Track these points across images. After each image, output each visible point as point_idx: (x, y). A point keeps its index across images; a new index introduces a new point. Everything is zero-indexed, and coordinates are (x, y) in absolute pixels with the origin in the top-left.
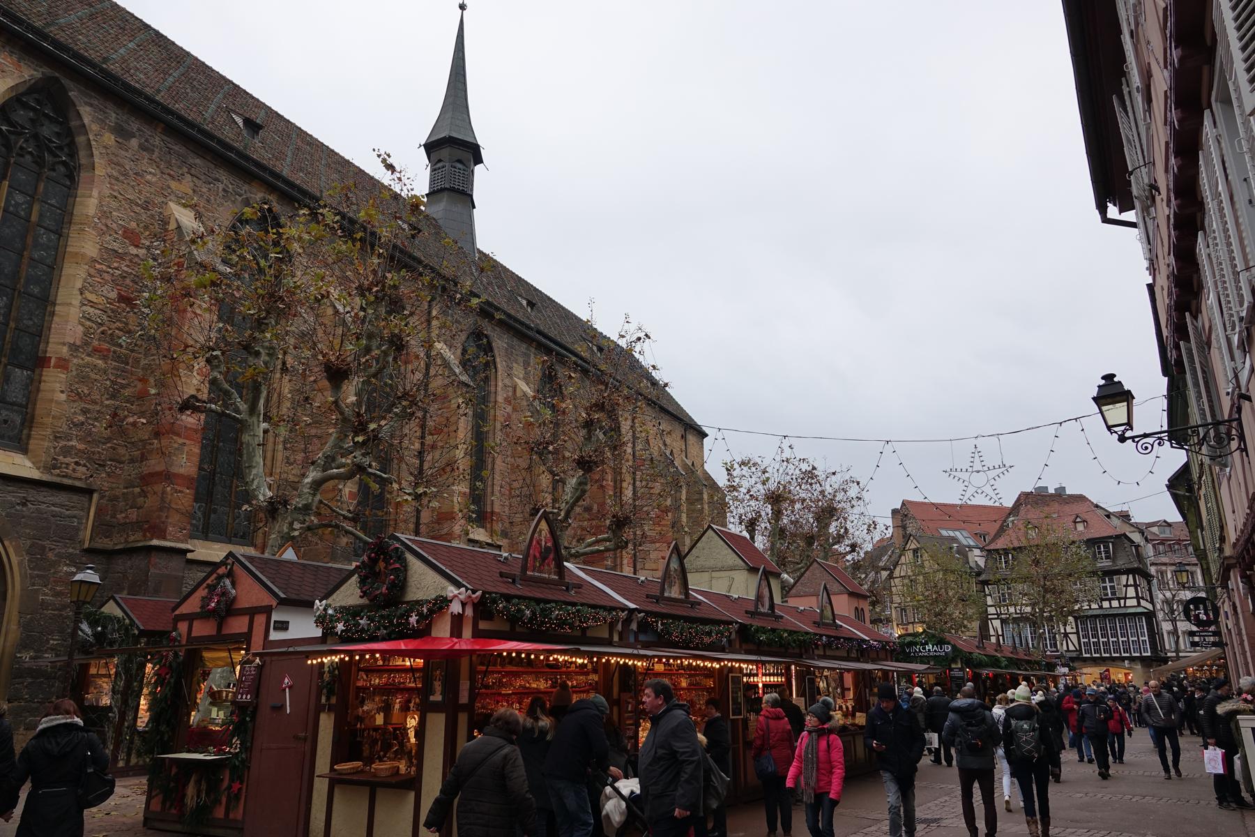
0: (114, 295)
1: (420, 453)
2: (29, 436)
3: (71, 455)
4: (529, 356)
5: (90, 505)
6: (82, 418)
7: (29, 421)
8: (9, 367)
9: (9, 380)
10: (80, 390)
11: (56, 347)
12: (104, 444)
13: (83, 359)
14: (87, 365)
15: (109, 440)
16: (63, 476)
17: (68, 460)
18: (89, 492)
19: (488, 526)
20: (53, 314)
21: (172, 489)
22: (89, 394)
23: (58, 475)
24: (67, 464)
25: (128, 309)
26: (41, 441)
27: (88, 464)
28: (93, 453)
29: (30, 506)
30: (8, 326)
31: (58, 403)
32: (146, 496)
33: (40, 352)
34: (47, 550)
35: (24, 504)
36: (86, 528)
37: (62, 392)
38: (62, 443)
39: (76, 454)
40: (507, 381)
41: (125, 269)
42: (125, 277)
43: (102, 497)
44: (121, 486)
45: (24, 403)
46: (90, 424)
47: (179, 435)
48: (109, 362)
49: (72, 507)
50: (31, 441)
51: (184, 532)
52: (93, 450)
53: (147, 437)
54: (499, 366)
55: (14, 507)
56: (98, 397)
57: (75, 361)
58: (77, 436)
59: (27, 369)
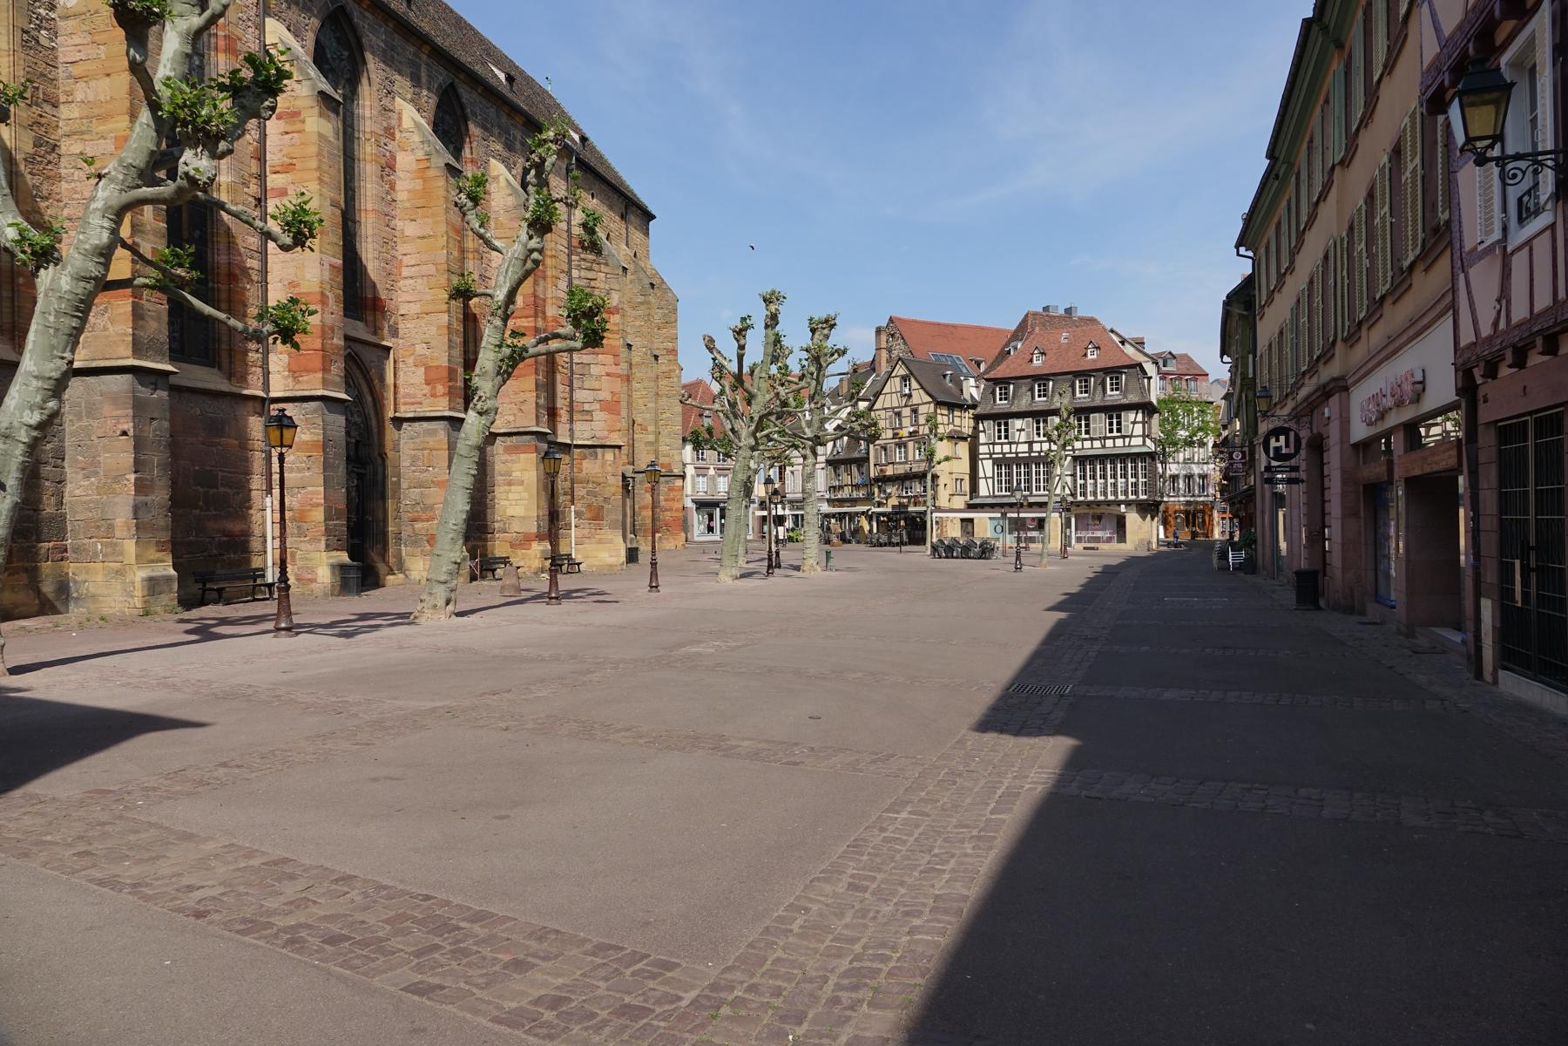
4: (419, 68)
19: (370, 318)
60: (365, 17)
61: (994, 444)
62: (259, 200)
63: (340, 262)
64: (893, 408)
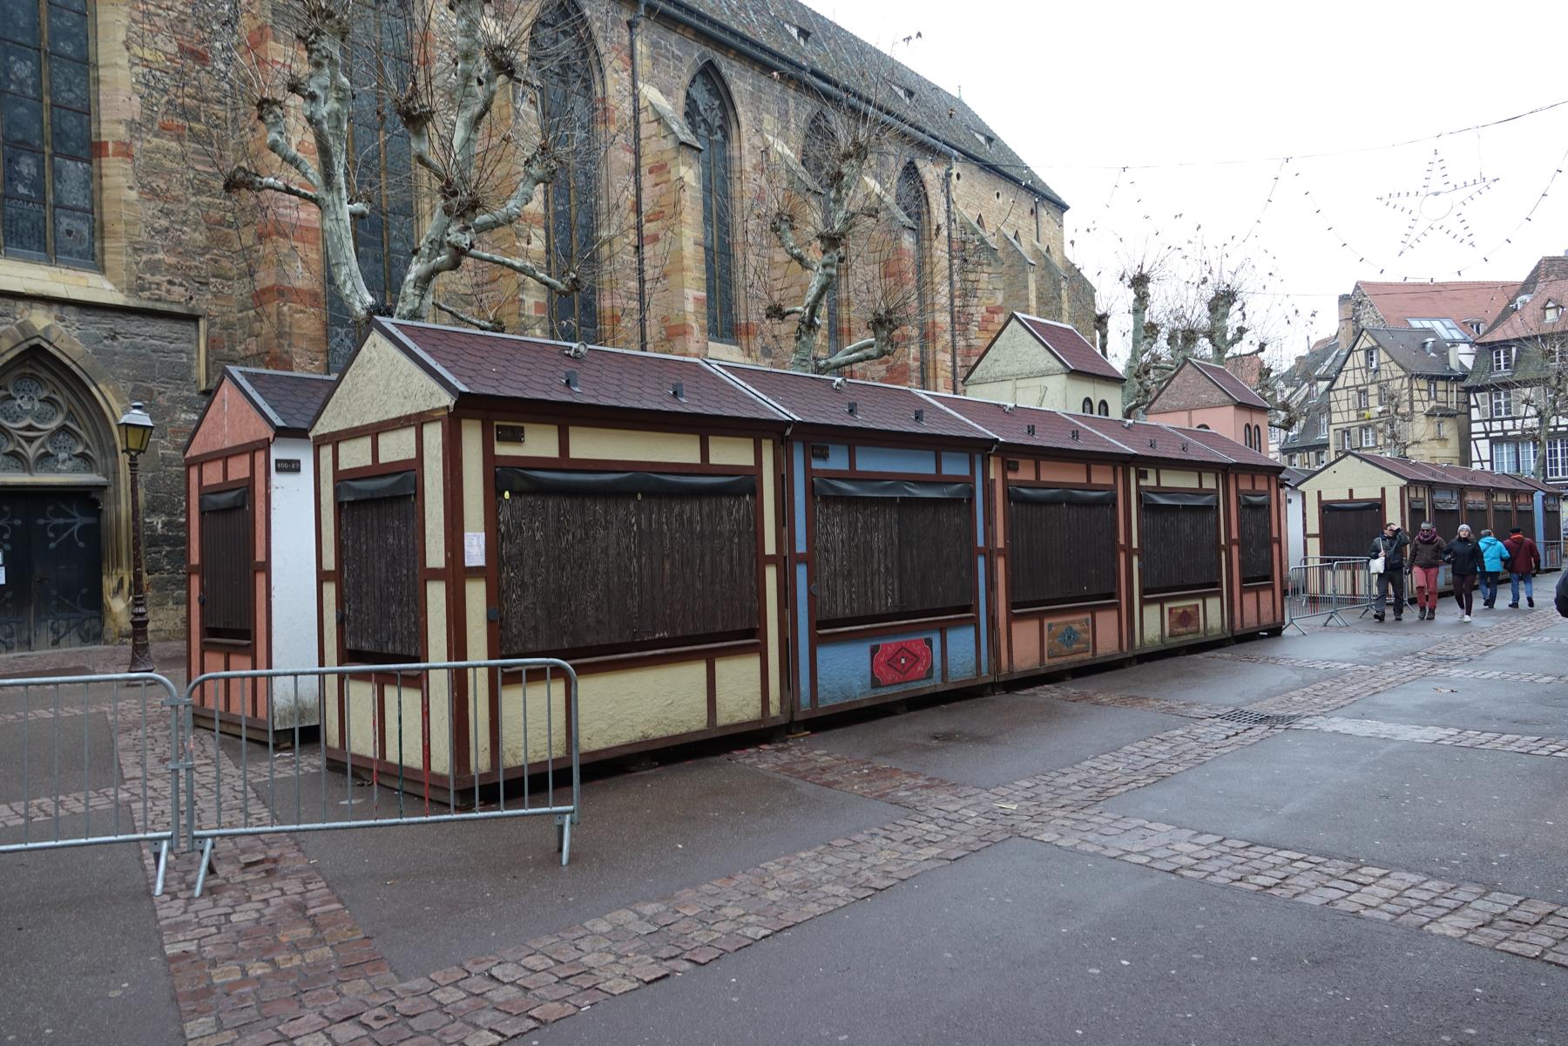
0: (172, 48)
1: (637, 248)
2: (103, 250)
3: (160, 272)
5: (198, 335)
6: (164, 222)
7: (98, 230)
8: (57, 159)
9: (60, 176)
10: (154, 185)
11: (111, 129)
12: (202, 255)
13: (149, 141)
14: (157, 150)
15: (206, 249)
16: (157, 300)
17: (157, 278)
18: (193, 318)
19: (744, 342)
20: (97, 80)
21: (290, 308)
22: (168, 190)
23: (149, 299)
24: (158, 284)
25: (197, 67)
26: (116, 251)
27: (184, 283)
28: (190, 268)
29: (121, 339)
30: (42, 101)
31: (128, 203)
32: (261, 321)
33: (93, 136)
34: (156, 393)
35: (114, 338)
36: (198, 364)
37: (131, 188)
38: (145, 257)
39: (167, 270)
40: (757, 141)
41: (181, 8)
42: (185, 21)
43: (213, 325)
44: (235, 310)
45: (88, 207)
46: (177, 230)
47: (286, 236)
48: (187, 143)
49: (177, 339)
50: (106, 257)
51: (317, 363)
52: (188, 263)
53: (251, 243)
54: (742, 119)
55: (101, 342)
56: (181, 193)
57: (139, 144)
58: (163, 247)
59: (83, 160)
60: (732, 66)
61: (1491, 420)
62: (637, 248)
63: (704, 294)
64: (1357, 387)
